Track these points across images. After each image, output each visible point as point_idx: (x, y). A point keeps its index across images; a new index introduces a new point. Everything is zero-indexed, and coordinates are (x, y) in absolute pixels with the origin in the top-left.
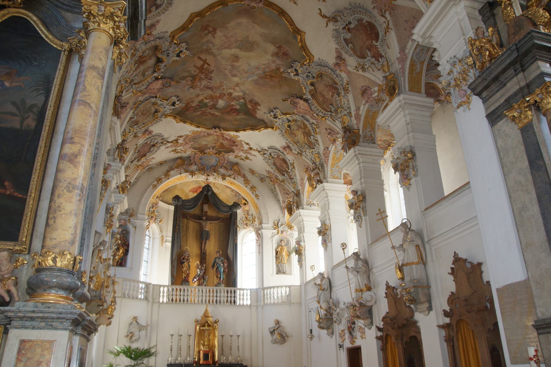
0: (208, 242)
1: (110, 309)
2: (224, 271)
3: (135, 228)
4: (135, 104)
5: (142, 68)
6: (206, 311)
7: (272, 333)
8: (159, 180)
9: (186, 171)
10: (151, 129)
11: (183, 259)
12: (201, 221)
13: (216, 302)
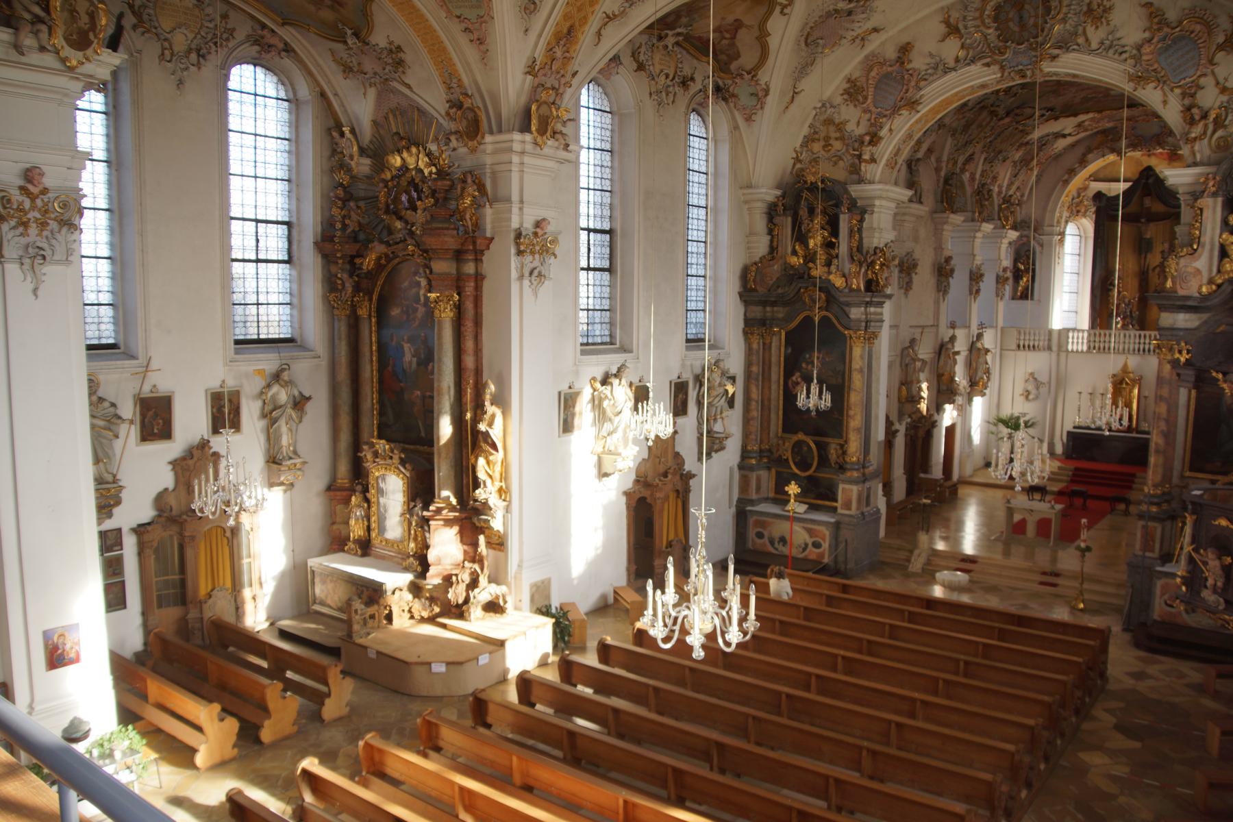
0: (1149, 256)
3: (1042, 246)
4: (985, 147)
5: (974, 127)
6: (1125, 365)
8: (1072, 172)
9: (1113, 150)
10: (1026, 140)
12: (1140, 225)
13: (1144, 350)
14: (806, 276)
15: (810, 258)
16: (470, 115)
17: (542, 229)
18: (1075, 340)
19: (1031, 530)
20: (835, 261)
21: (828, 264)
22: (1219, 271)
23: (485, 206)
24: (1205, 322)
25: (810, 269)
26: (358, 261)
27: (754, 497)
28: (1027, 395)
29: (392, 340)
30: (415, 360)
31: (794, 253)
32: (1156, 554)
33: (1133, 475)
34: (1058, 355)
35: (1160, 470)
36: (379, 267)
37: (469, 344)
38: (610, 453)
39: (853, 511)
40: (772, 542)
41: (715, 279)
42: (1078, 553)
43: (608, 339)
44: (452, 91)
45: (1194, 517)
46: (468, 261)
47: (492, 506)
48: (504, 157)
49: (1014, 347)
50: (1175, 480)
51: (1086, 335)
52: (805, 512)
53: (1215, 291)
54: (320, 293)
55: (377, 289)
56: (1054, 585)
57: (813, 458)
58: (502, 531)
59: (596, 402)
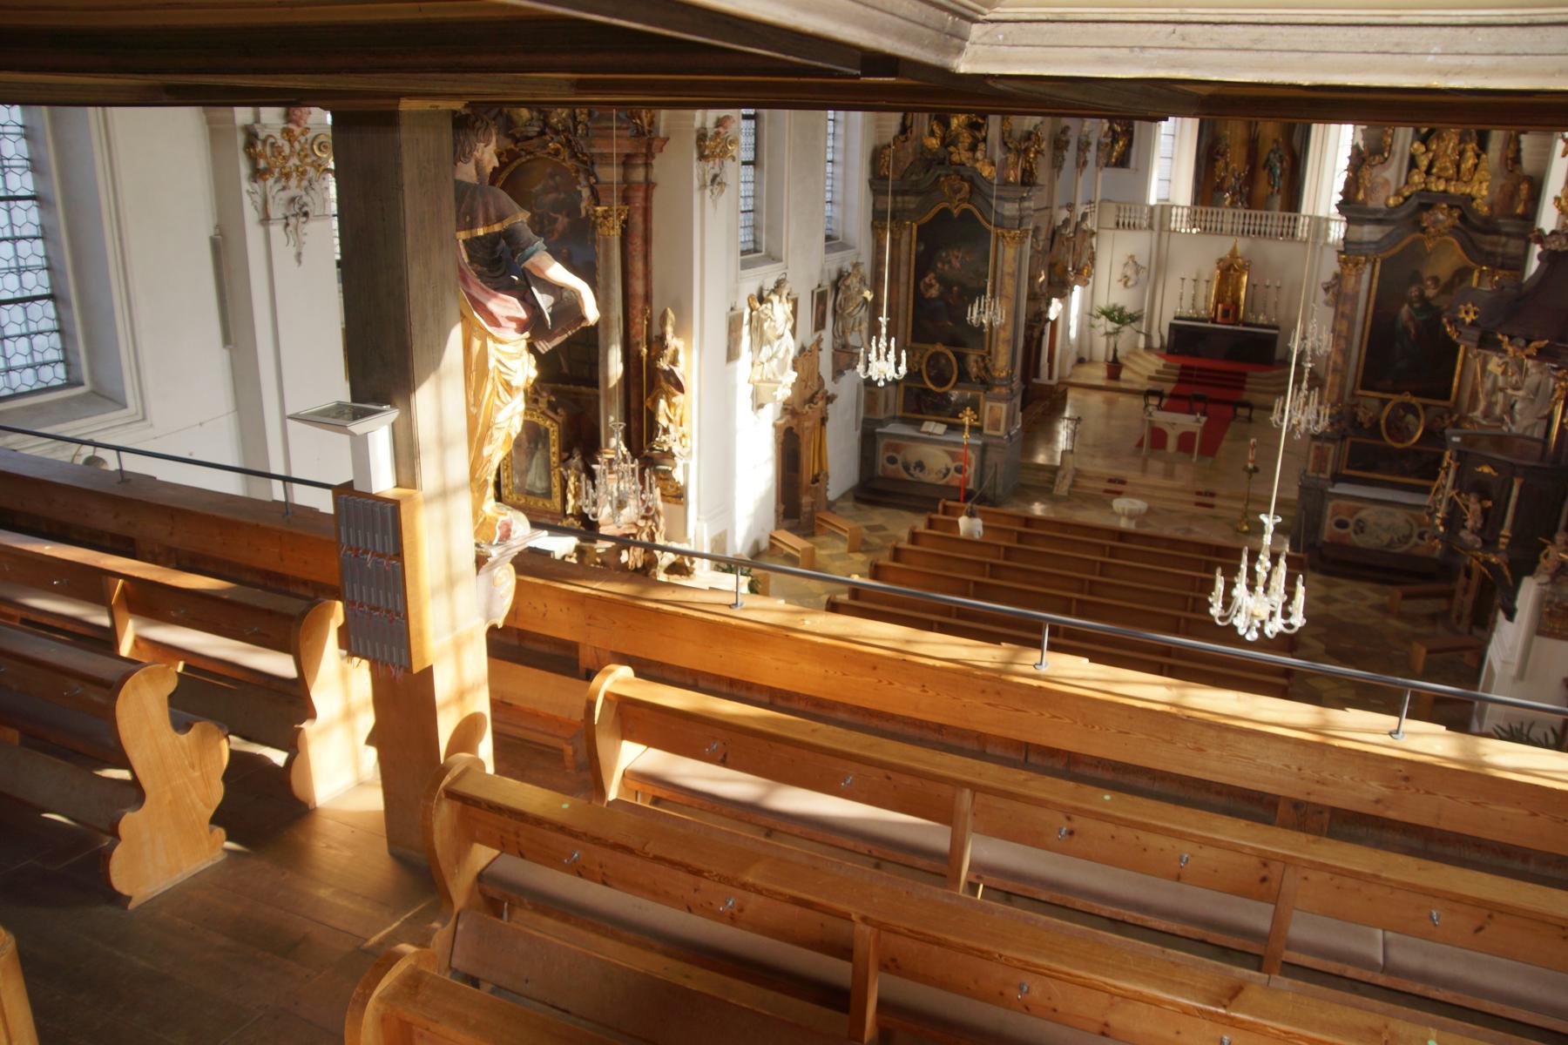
1: (1086, 271)
2: (1281, 175)
6: (1235, 248)
7: (1326, 290)
11: (1218, 153)
14: (947, 163)
15: (948, 141)
17: (725, 128)
18: (1179, 219)
19: (1172, 444)
20: (981, 146)
21: (973, 148)
22: (1407, 183)
24: (1388, 236)
25: (951, 153)
27: (882, 416)
28: (1125, 280)
31: (932, 133)
32: (1327, 475)
33: (1245, 375)
34: (1160, 235)
35: (1336, 390)
37: (638, 266)
38: (769, 381)
39: (1001, 432)
40: (906, 468)
41: (846, 164)
42: (1245, 474)
43: (751, 246)
45: (1458, 464)
46: (636, 166)
47: (676, 454)
49: (1113, 225)
50: (1346, 399)
51: (1186, 211)
52: (945, 433)
53: (1402, 204)
56: (1211, 506)
57: (952, 373)
58: (682, 484)
59: (754, 323)
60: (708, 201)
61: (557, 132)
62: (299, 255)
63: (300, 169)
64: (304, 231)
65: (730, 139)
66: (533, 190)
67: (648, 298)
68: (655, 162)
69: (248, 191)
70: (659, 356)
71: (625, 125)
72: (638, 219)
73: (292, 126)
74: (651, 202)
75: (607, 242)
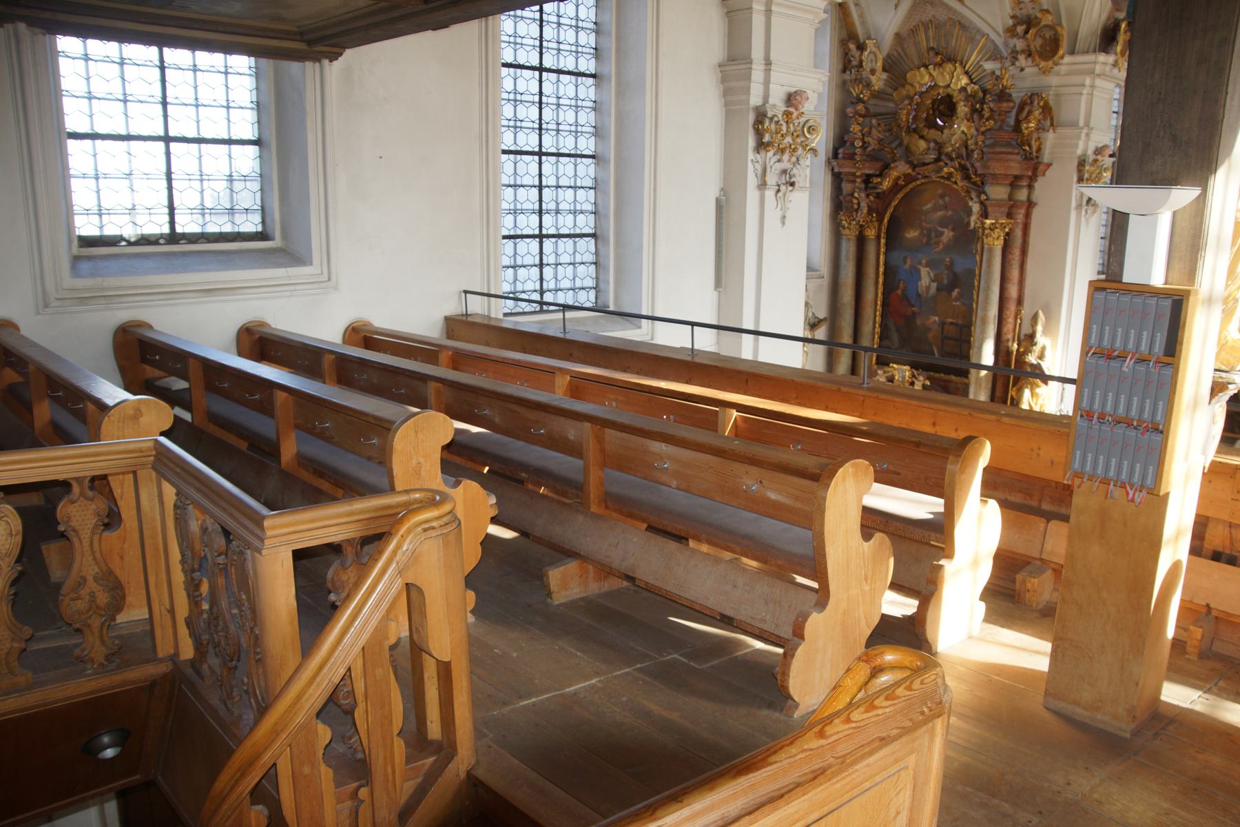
16: (1048, 34)
23: (1048, 131)
26: (876, 180)
29: (905, 263)
30: (934, 285)
36: (896, 188)
37: (1015, 273)
44: (1022, 6)
46: (1021, 187)
48: (1076, 79)
54: (828, 213)
55: (891, 210)
60: (1083, 219)
61: (952, 159)
62: (784, 217)
63: (793, 147)
64: (790, 199)
65: (1105, 166)
66: (924, 208)
67: (1020, 302)
68: (1037, 185)
69: (752, 160)
70: (1028, 351)
71: (1016, 151)
72: (1018, 233)
73: (791, 109)
74: (1030, 219)
75: (991, 250)
